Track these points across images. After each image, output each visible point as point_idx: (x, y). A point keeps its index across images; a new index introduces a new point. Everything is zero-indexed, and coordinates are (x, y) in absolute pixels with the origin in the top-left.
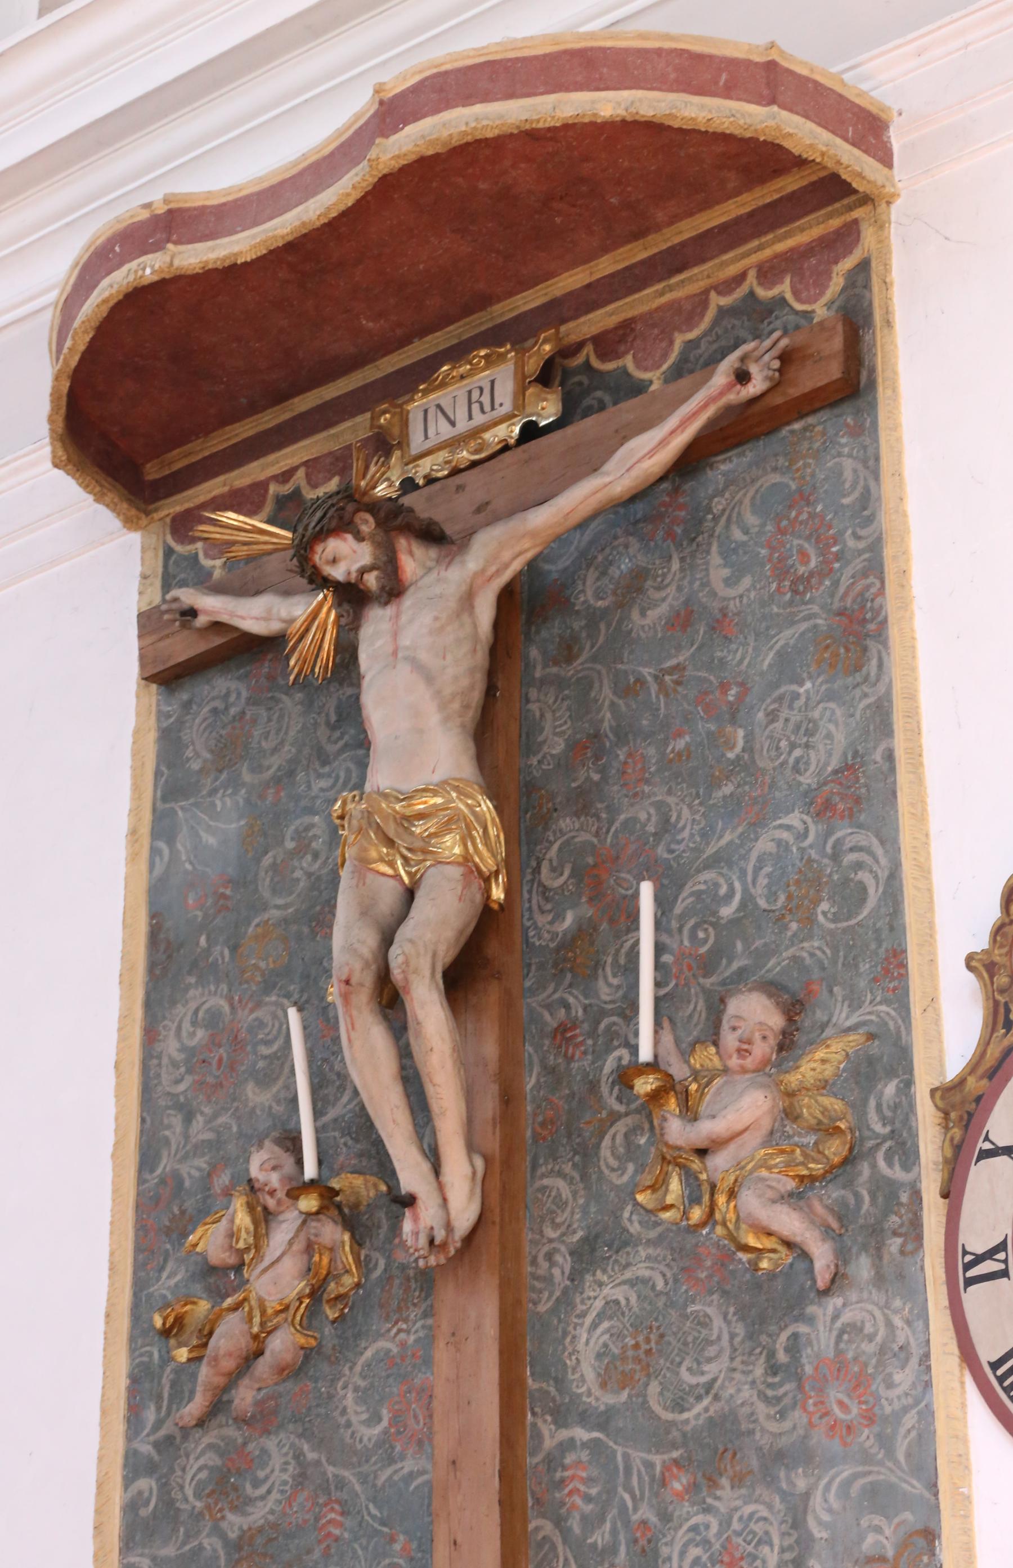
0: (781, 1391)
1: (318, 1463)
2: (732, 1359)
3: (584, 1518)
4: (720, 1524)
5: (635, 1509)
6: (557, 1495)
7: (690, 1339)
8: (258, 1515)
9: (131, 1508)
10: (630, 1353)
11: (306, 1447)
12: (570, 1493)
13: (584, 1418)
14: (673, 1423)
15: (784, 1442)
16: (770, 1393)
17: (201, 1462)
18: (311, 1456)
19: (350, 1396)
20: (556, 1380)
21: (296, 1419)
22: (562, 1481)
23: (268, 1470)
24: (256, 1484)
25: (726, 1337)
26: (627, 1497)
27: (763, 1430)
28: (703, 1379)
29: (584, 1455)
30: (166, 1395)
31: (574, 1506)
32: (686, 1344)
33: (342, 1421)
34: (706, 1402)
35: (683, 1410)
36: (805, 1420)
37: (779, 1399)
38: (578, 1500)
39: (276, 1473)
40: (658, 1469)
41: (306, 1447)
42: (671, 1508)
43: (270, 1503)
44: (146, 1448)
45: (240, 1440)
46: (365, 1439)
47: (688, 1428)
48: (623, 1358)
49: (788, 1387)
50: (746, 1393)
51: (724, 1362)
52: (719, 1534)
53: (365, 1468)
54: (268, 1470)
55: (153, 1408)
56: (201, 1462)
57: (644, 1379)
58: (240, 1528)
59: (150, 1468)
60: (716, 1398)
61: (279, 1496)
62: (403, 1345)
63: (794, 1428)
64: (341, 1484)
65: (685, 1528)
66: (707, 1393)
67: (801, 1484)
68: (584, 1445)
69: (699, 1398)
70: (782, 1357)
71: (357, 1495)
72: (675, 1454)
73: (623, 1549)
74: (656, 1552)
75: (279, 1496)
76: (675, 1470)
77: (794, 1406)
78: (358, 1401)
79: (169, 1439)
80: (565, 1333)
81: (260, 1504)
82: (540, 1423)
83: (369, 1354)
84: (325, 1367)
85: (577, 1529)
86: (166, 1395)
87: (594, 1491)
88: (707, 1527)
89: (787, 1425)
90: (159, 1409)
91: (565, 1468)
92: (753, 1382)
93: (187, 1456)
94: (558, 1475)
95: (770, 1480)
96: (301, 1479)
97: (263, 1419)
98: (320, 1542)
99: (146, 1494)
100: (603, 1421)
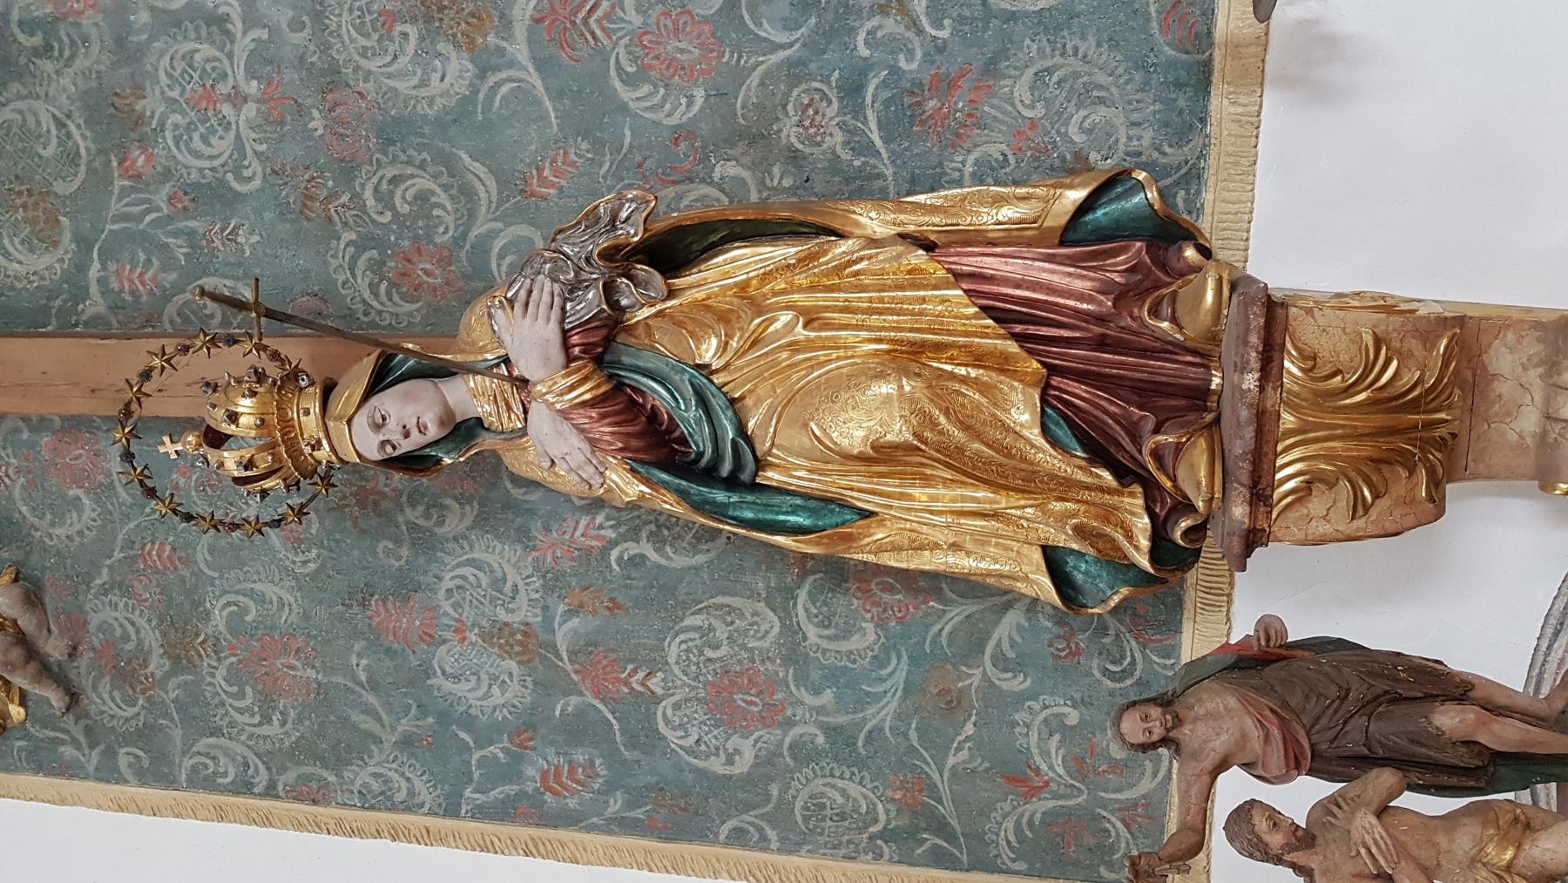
0: (66, 39)
1: (110, 568)
2: (38, 97)
3: (165, 268)
4: (174, 111)
5: (158, 209)
6: (144, 298)
7: (20, 146)
8: (152, 638)
9: (144, 777)
10: (30, 214)
11: (98, 582)
12: (143, 283)
13: (81, 267)
14: (89, 163)
15: (109, 41)
16: (67, 54)
17: (106, 697)
18: (105, 576)
19: (58, 531)
20: (49, 299)
21: (75, 594)
22: (133, 293)
23: (116, 624)
24: (126, 638)
25: (20, 104)
26: (148, 219)
27: (98, 62)
28: (53, 129)
29: (112, 267)
30: (52, 734)
31: (154, 279)
32: (24, 150)
33: (78, 539)
34: (72, 128)
35: (78, 155)
36: (90, 12)
37: (73, 42)
38: (149, 274)
39: (118, 615)
40: (127, 183)
41: (98, 582)
42: (159, 169)
43: (142, 622)
44: (95, 756)
45: (91, 655)
46: (94, 515)
47: (93, 147)
48: (33, 222)
49: (62, 34)
50: (66, 81)
51: (40, 106)
52: (183, 113)
53: (116, 516)
54: (116, 624)
55: (62, 749)
56: (106, 697)
57: (52, 199)
58: (161, 656)
59: (110, 753)
60: (69, 116)
61: (137, 612)
62: (18, 471)
63: (96, 25)
64: (129, 544)
65: (175, 151)
66: (65, 126)
67: (144, 17)
68: (104, 268)
69: (69, 135)
70: (37, 40)
71: (138, 526)
72: (115, 164)
73: (193, 224)
74: (196, 186)
75: (137, 612)
76: (128, 163)
77: (77, 25)
78: (62, 524)
79: (88, 731)
80: (13, 288)
81: (142, 635)
82: (84, 318)
83: (24, 509)
84: (34, 558)
85: (173, 276)
86: (52, 734)
87: (142, 256)
88: (176, 126)
89: (94, 34)
90: (63, 742)
91: (122, 291)
92: (57, 72)
93: (103, 712)
94: (129, 298)
95: (142, 50)
96: (124, 588)
97: (76, 626)
98: (176, 569)
99: (131, 759)
100: (84, 243)
